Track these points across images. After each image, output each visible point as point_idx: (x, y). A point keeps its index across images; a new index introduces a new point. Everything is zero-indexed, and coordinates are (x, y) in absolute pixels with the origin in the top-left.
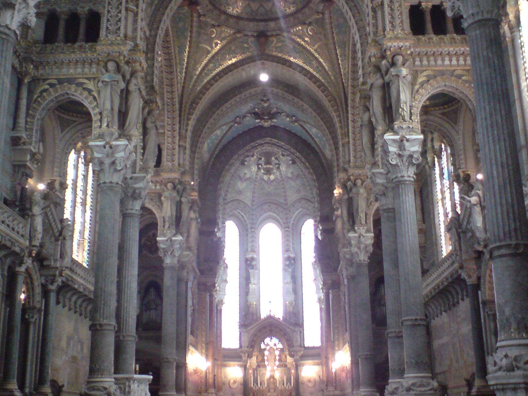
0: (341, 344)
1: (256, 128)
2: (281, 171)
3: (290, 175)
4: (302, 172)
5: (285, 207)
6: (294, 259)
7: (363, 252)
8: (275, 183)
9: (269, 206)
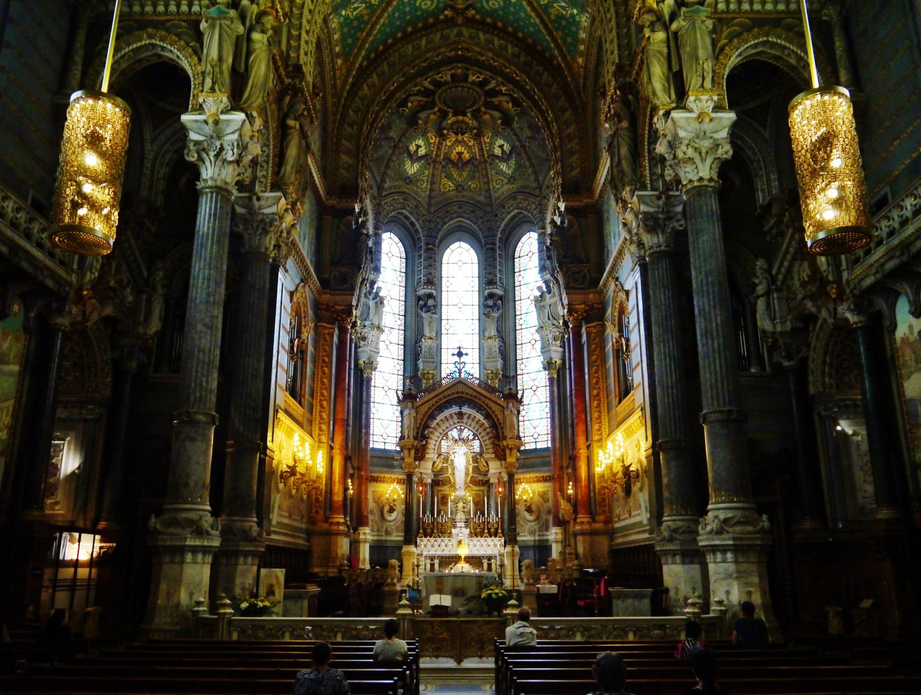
0: (605, 430)
1: (437, 22)
2: (480, 144)
3: (497, 151)
4: (519, 141)
5: (489, 209)
6: (501, 298)
7: (709, 160)
8: (469, 168)
9: (460, 207)
